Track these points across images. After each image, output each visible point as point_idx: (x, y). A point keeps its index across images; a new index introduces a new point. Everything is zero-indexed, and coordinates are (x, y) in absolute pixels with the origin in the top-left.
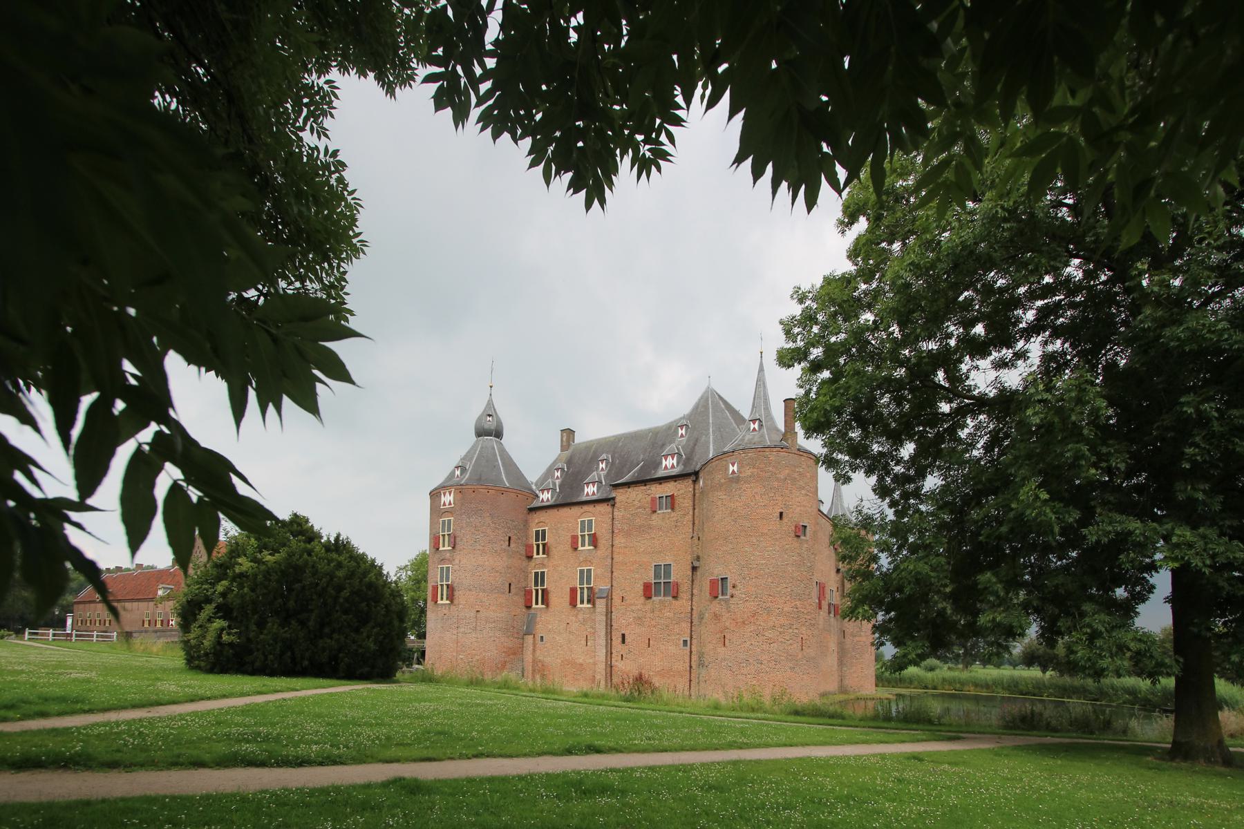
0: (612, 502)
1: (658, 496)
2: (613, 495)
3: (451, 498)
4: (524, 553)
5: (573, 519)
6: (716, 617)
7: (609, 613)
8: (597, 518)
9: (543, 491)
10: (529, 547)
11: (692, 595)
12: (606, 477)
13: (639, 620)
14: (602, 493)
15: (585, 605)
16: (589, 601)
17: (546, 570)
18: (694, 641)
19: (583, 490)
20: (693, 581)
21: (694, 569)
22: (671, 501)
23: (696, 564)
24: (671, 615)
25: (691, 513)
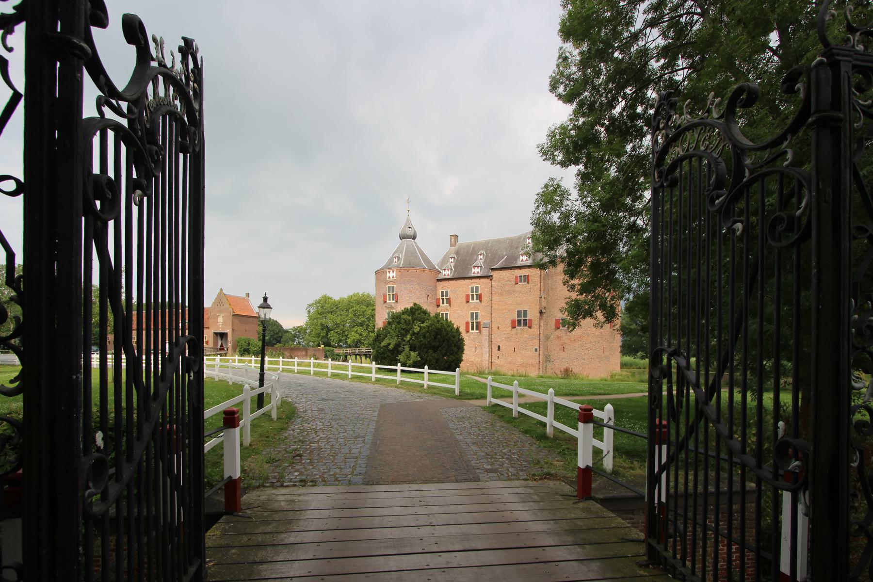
0: (491, 278)
1: (519, 275)
2: (491, 274)
3: (394, 274)
4: (435, 303)
5: (465, 286)
6: (559, 337)
7: (490, 335)
8: (482, 286)
9: (445, 270)
10: (438, 300)
11: (540, 326)
13: (509, 339)
14: (483, 272)
15: (475, 331)
17: (449, 313)
18: (541, 349)
21: (541, 313)
22: (527, 279)
23: (543, 311)
25: (539, 285)
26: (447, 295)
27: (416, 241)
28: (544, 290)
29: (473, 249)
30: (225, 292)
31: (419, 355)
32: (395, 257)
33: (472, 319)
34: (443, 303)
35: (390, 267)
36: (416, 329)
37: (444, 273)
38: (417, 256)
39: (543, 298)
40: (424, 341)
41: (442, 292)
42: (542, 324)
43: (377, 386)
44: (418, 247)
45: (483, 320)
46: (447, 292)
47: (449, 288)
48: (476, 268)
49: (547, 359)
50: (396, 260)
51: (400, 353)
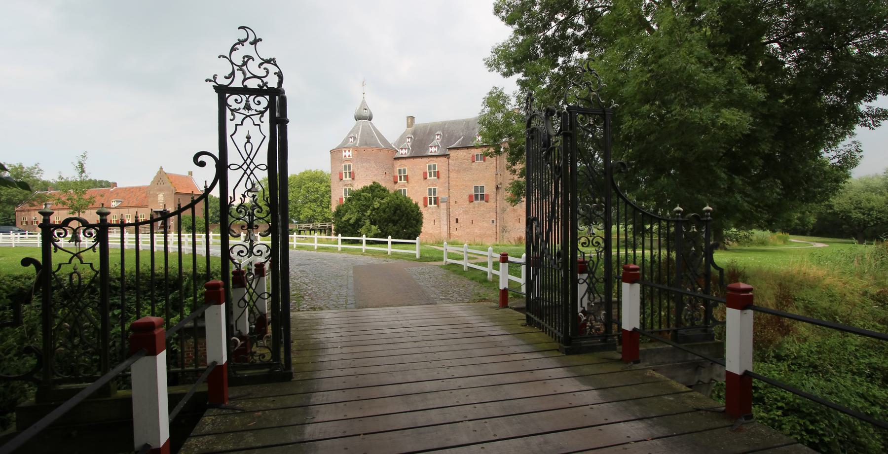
0: (448, 156)
2: (449, 153)
5: (423, 164)
7: (448, 209)
8: (440, 164)
9: (402, 149)
10: (395, 177)
11: (496, 200)
13: (466, 212)
15: (433, 205)
16: (435, 204)
17: (406, 189)
18: (498, 221)
20: (496, 194)
21: (497, 188)
23: (499, 186)
24: (485, 209)
27: (372, 121)
28: (500, 167)
29: (431, 129)
30: (166, 170)
31: (380, 228)
32: (351, 137)
33: (430, 194)
34: (401, 180)
35: (346, 146)
36: (376, 205)
37: (401, 152)
39: (499, 175)
40: (385, 216)
41: (400, 170)
42: (498, 198)
43: (345, 255)
44: (374, 128)
45: (441, 195)
46: (404, 170)
47: (408, 166)
48: (433, 147)
49: (504, 230)
50: (352, 140)
51: (361, 226)
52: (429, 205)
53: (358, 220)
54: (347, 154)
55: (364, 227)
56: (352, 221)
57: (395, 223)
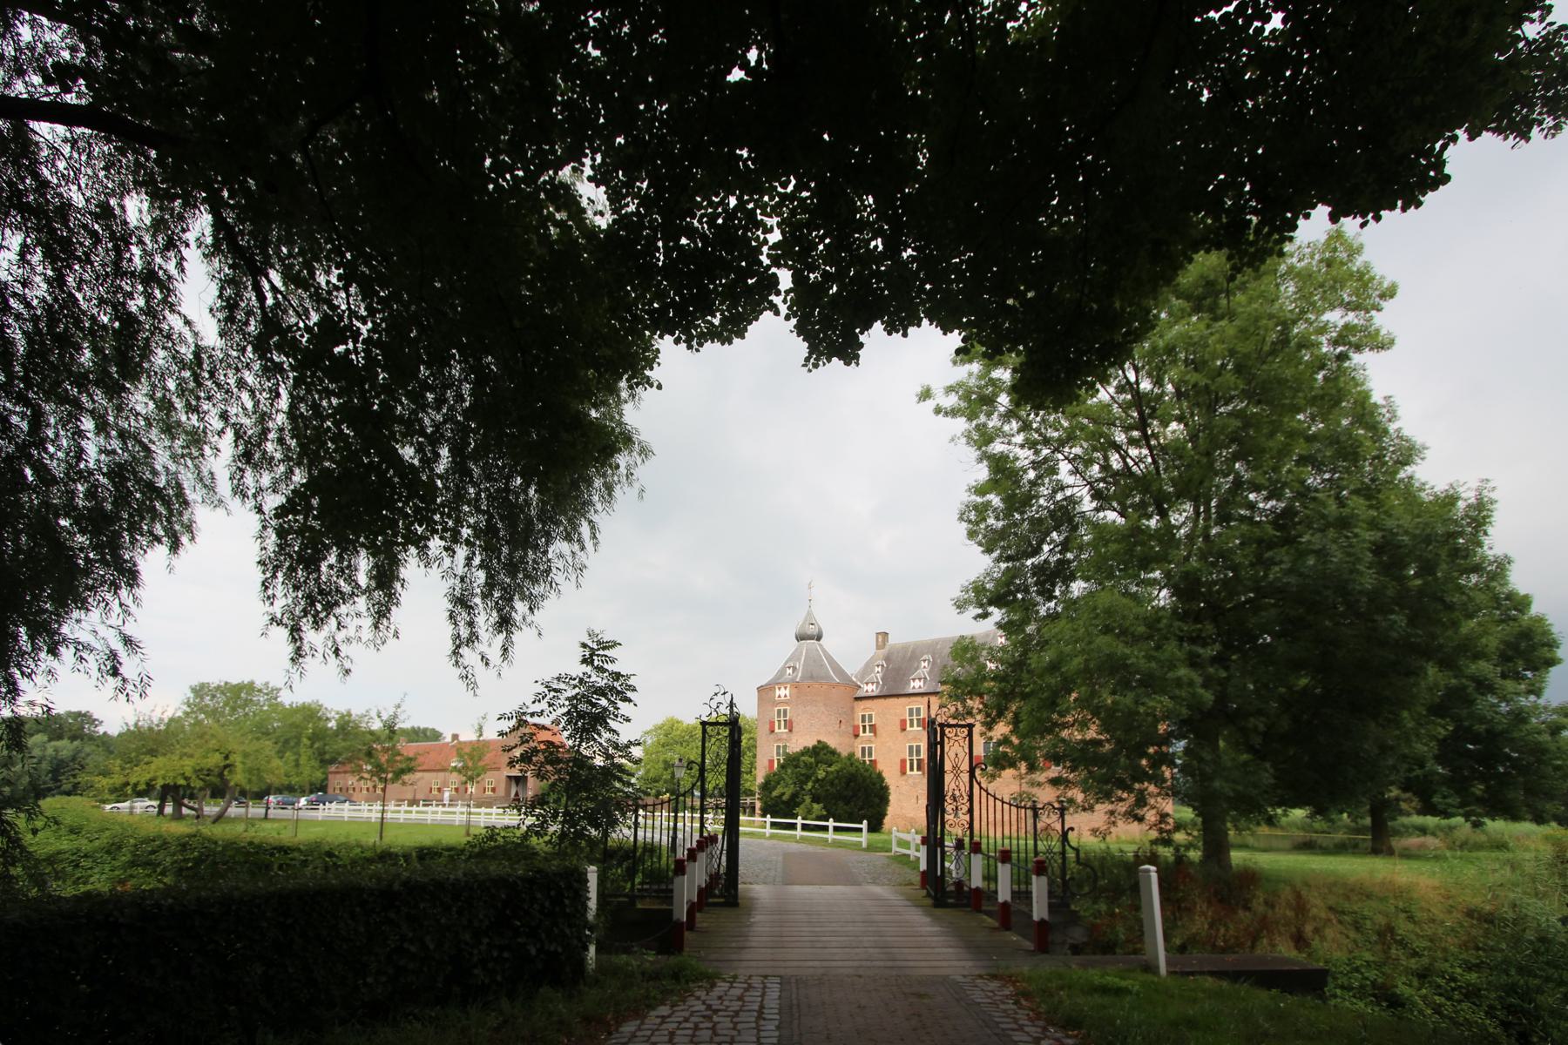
5: (901, 707)
10: (856, 728)
12: (929, 673)
19: (909, 684)
26: (870, 720)
29: (913, 652)
33: (911, 754)
34: (864, 731)
38: (822, 665)
41: (863, 716)
43: (774, 842)
44: (825, 651)
46: (870, 716)
47: (875, 710)
50: (790, 671)
51: (798, 805)
52: (908, 772)
53: (794, 796)
54: (782, 692)
55: (802, 806)
56: (785, 798)
57: (847, 801)
